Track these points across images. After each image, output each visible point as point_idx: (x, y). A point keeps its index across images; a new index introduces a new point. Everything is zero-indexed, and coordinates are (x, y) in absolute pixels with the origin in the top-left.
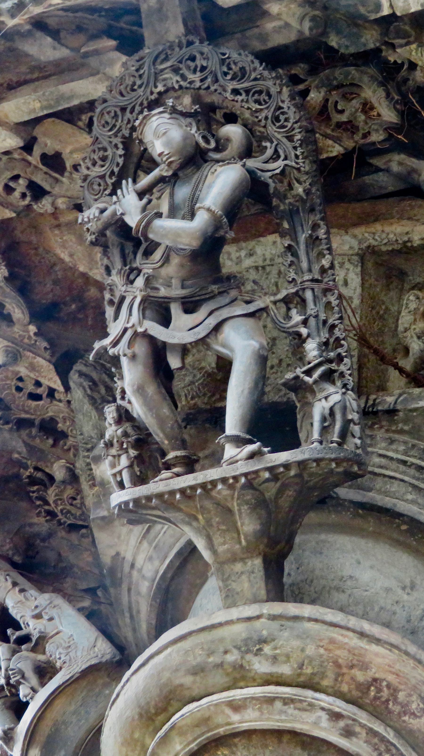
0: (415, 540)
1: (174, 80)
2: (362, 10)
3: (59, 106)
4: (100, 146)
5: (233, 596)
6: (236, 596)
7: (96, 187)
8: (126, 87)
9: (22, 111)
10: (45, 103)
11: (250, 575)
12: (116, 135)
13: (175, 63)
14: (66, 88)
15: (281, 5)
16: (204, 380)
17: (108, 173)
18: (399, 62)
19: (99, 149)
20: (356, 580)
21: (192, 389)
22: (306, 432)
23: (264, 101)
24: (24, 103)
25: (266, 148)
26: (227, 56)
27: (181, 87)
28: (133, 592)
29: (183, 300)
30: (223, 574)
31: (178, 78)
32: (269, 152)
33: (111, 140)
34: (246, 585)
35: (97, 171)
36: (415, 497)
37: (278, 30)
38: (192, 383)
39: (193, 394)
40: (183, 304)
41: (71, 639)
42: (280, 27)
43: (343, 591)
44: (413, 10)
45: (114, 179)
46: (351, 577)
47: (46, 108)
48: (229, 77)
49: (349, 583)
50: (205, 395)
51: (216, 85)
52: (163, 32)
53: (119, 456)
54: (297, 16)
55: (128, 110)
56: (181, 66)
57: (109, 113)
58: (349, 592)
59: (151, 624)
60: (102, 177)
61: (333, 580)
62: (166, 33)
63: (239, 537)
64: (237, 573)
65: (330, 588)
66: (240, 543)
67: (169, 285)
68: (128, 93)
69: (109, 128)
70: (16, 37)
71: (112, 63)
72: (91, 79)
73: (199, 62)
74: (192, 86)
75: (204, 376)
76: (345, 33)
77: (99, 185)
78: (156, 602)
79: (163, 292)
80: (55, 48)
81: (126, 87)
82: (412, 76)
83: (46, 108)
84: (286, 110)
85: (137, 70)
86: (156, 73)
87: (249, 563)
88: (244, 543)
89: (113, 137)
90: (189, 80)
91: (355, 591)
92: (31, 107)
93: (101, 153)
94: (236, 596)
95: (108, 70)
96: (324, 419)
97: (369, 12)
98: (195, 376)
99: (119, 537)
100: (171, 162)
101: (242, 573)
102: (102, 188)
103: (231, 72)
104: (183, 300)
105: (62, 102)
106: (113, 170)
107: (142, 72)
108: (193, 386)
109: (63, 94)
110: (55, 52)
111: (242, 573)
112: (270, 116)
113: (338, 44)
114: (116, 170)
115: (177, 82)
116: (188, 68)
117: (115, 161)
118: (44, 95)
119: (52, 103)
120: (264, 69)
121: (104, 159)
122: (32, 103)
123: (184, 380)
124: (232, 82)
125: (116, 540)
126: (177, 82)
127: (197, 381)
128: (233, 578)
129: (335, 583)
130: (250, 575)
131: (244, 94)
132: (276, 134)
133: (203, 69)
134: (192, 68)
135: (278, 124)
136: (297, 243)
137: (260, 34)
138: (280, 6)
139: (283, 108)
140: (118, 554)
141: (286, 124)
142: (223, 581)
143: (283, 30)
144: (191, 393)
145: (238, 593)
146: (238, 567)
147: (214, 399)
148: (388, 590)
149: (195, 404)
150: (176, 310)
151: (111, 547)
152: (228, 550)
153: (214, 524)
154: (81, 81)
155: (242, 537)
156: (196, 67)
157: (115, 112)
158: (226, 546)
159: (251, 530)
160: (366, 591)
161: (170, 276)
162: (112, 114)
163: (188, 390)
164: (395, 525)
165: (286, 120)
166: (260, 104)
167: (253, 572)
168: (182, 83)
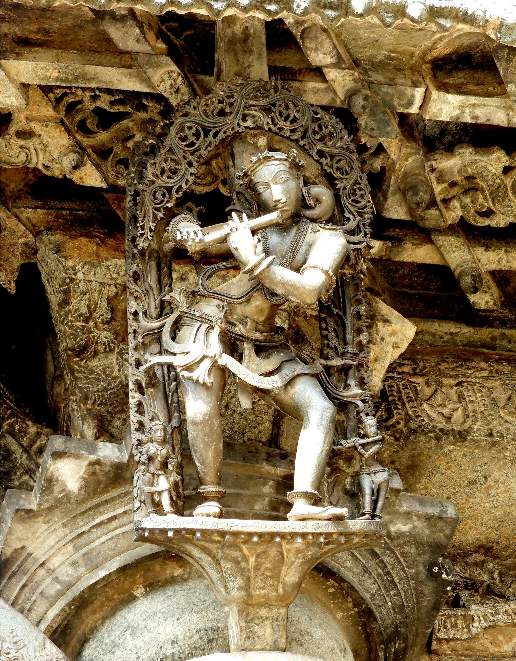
0: (334, 603)
1: (264, 120)
2: (396, 102)
3: (74, 83)
4: (173, 157)
5: (254, 638)
6: (256, 639)
7: (159, 196)
8: (213, 110)
9: (36, 74)
10: (63, 75)
11: (273, 622)
12: (193, 153)
13: (268, 104)
14: (91, 69)
15: (339, 73)
16: (118, 390)
17: (175, 188)
18: (368, 146)
19: (173, 160)
20: (311, 636)
21: (103, 395)
22: (337, 497)
23: (346, 171)
24: (43, 68)
25: (349, 219)
26: (319, 116)
27: (270, 129)
28: (27, 589)
29: (257, 343)
30: (247, 616)
31: (270, 121)
32: (351, 225)
33: (187, 156)
34: (269, 631)
35: (164, 181)
36: (351, 565)
37: (315, 91)
38: (105, 390)
39: (102, 401)
40: (255, 345)
41: (14, 634)
42: (319, 90)
43: (301, 645)
44: (441, 119)
45: (180, 195)
46: (308, 633)
47: (61, 80)
48: (318, 137)
49: (306, 637)
50: (111, 404)
51: (305, 140)
52: (246, 65)
53: (159, 475)
54: (346, 88)
55: (211, 134)
56: (273, 109)
57: (190, 128)
58: (306, 646)
59: (52, 627)
60: (169, 190)
61: (294, 632)
62: (249, 67)
63: (278, 586)
64: (262, 617)
65: (292, 639)
66: (277, 590)
67: (244, 324)
68: (213, 115)
69: (187, 143)
70: (107, 17)
71: (158, 65)
72: (121, 70)
73: (292, 113)
74: (282, 133)
75: (118, 385)
76: (377, 118)
77: (164, 195)
78: (70, 608)
79: (240, 329)
80: (138, 41)
81: (213, 110)
82: (372, 161)
83: (61, 80)
84: (363, 186)
85: (228, 97)
86: (245, 106)
87: (275, 611)
88: (281, 591)
89: (188, 153)
90: (278, 126)
91: (311, 646)
92: (48, 74)
93: (173, 165)
94: (256, 639)
95: (150, 71)
96: (373, 494)
97: (400, 105)
98: (109, 384)
99: (34, 533)
100: (285, 210)
101: (267, 618)
102: (166, 199)
103: (321, 133)
104: (257, 343)
105: (80, 81)
106: (181, 185)
107: (232, 100)
108: (105, 393)
109: (86, 74)
110: (137, 44)
111: (267, 618)
112: (348, 188)
113: (366, 123)
114: (184, 186)
115: (268, 123)
116: (280, 114)
117: (186, 178)
118: (67, 68)
119: (70, 77)
120: (351, 142)
121: (175, 172)
122: (51, 71)
123: (98, 385)
124: (319, 143)
125: (29, 535)
126: (268, 123)
127: (111, 389)
128: (256, 621)
129: (296, 635)
130: (273, 622)
131: (329, 159)
132: (350, 206)
133: (294, 120)
134: (285, 115)
135: (353, 198)
136: (345, 314)
137: (299, 89)
138: (337, 75)
139: (360, 184)
140: (23, 548)
141: (360, 199)
142: (246, 622)
143: (320, 92)
144: (101, 399)
145: (258, 637)
146: (264, 612)
147: (117, 409)
148: (332, 650)
149: (99, 411)
150: (248, 349)
151: (20, 540)
152: (264, 596)
153: (262, 569)
154: (110, 69)
155: (281, 585)
156: (288, 116)
157: (197, 130)
158: (264, 590)
159: (291, 582)
160: (319, 648)
161: (246, 315)
162: (194, 131)
163: (99, 395)
164: (324, 587)
165: (362, 196)
166: (343, 174)
167: (277, 620)
168: (271, 126)
